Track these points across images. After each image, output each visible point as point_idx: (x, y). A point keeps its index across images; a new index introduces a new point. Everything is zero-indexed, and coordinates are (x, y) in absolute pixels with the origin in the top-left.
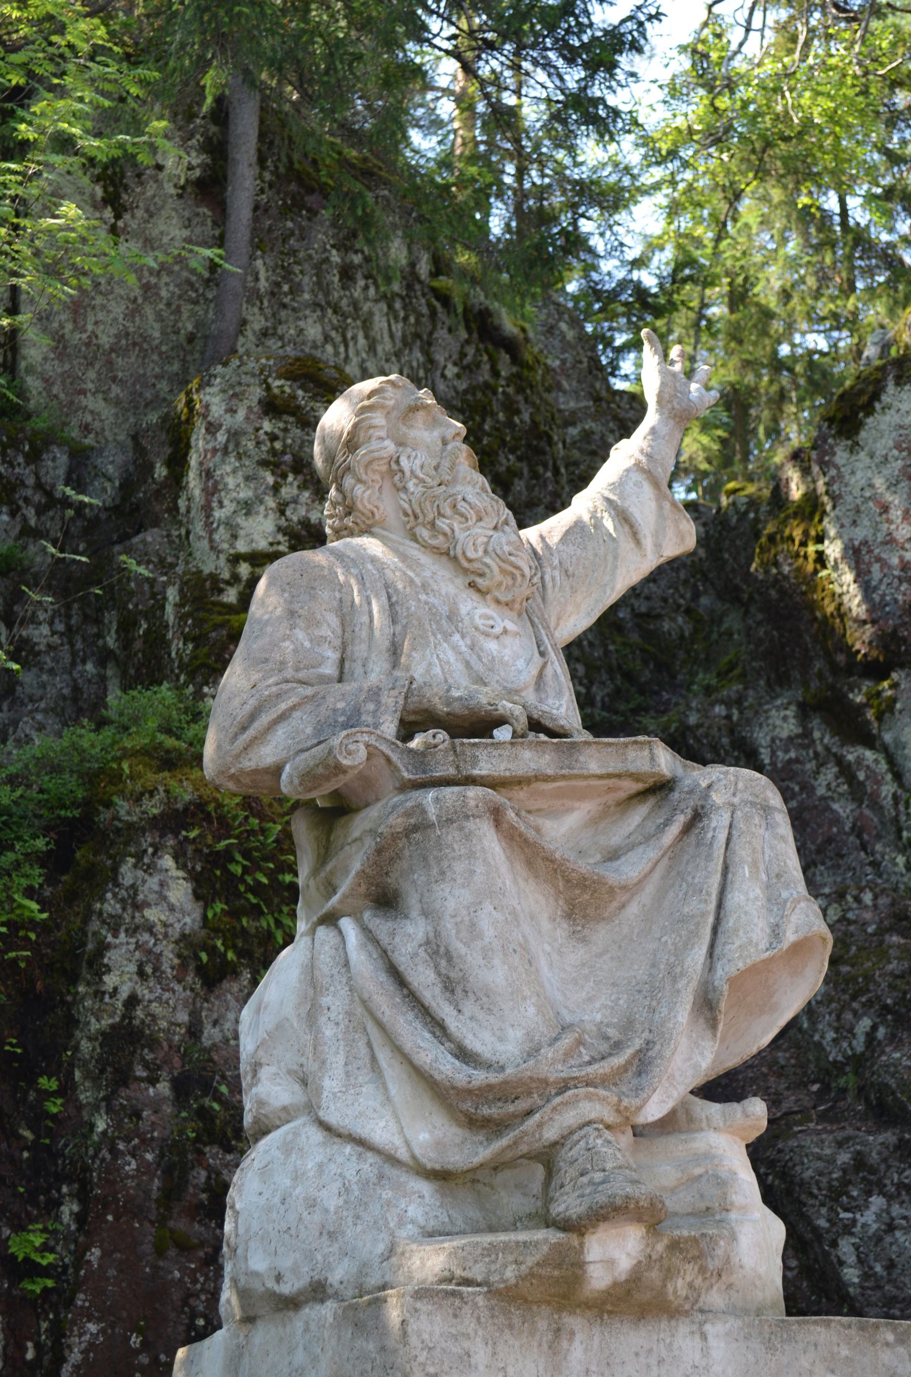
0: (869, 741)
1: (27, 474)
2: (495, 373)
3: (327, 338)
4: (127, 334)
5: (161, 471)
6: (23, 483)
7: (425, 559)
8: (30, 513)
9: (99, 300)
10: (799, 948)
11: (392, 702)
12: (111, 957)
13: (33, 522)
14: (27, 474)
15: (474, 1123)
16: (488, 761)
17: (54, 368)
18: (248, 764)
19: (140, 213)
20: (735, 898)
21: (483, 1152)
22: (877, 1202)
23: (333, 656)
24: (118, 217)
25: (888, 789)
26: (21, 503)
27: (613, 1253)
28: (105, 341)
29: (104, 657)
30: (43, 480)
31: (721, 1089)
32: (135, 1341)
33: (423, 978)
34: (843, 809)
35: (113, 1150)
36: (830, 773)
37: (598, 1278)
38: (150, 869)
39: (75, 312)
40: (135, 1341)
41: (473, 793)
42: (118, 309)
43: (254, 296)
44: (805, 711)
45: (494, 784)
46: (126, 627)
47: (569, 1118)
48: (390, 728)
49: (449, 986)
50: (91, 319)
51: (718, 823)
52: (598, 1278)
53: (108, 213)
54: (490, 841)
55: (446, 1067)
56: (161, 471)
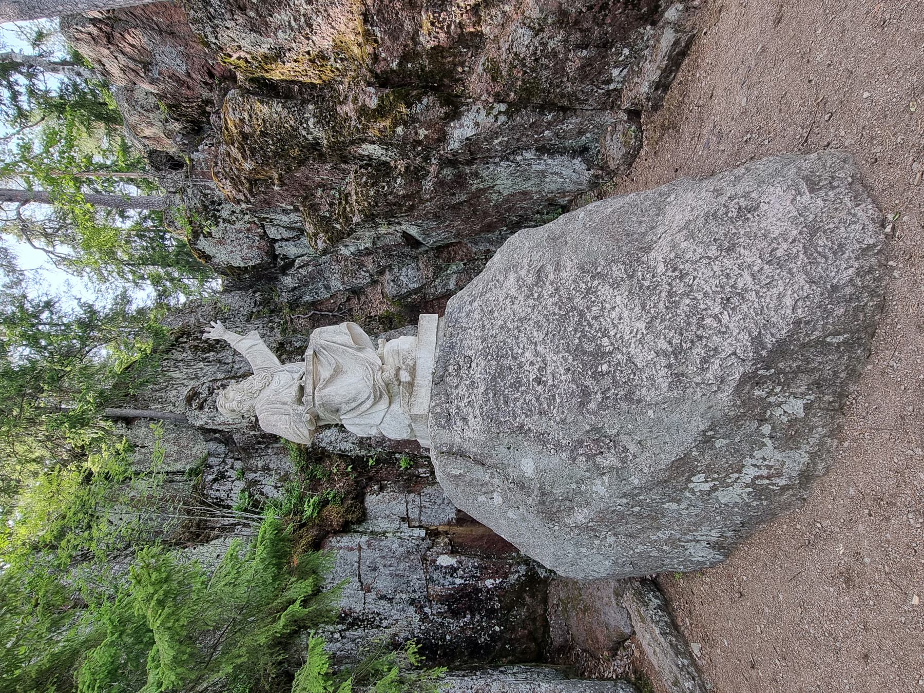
0: (294, 261)
1: (216, 469)
2: (186, 342)
3: (176, 389)
5: (217, 435)
7: (261, 395)
8: (227, 467)
10: (349, 328)
11: (295, 407)
12: (343, 448)
14: (216, 469)
15: (381, 397)
16: (309, 389)
17: (184, 462)
18: (308, 436)
20: (339, 342)
21: (386, 397)
22: (401, 278)
25: (305, 258)
27: (405, 376)
28: (176, 448)
29: (267, 447)
31: (376, 346)
33: (354, 405)
34: (310, 269)
36: (301, 270)
37: (409, 379)
41: (316, 394)
43: (163, 409)
44: (285, 274)
45: (314, 388)
46: (259, 443)
47: (380, 381)
48: (301, 408)
49: (354, 400)
51: (323, 342)
52: (409, 379)
53: (137, 449)
54: (326, 391)
55: (370, 401)
56: (217, 435)
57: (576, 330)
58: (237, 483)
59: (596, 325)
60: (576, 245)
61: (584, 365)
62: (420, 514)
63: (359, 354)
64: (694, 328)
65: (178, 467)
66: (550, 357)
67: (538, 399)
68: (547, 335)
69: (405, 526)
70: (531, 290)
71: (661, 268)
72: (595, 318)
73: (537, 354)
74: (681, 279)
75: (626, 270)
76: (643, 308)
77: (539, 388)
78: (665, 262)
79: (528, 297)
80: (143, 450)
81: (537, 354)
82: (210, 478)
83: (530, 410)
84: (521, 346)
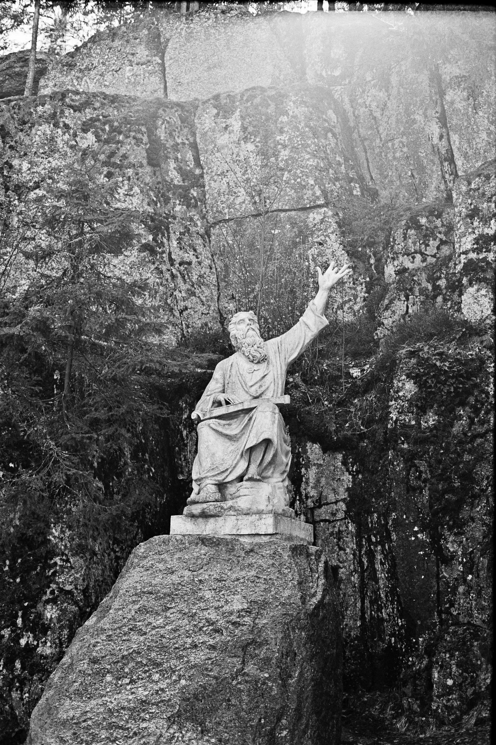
4: (490, 143)
6: (436, 227)
9: (475, 135)
13: (444, 239)
19: (485, 93)
23: (221, 385)
24: (475, 101)
26: (438, 235)
30: (445, 223)
32: (405, 517)
35: (393, 464)
38: (399, 381)
39: (469, 143)
40: (405, 517)
42: (484, 136)
50: (474, 143)
57: (150, 660)
58: (418, 257)
59: (143, 675)
60: (220, 665)
61: (118, 662)
62: (325, 521)
63: (238, 457)
64: (85, 738)
65: (459, 163)
66: (142, 638)
67: (120, 628)
68: (162, 636)
69: (310, 503)
70: (212, 624)
71: (144, 725)
72: (150, 676)
73: (154, 628)
74: (126, 736)
75: (162, 701)
76: (123, 708)
77: (126, 629)
78: (146, 728)
79: (208, 622)
80: (470, 109)
81: (154, 628)
82: (423, 221)
83: (115, 622)
84: (172, 616)
